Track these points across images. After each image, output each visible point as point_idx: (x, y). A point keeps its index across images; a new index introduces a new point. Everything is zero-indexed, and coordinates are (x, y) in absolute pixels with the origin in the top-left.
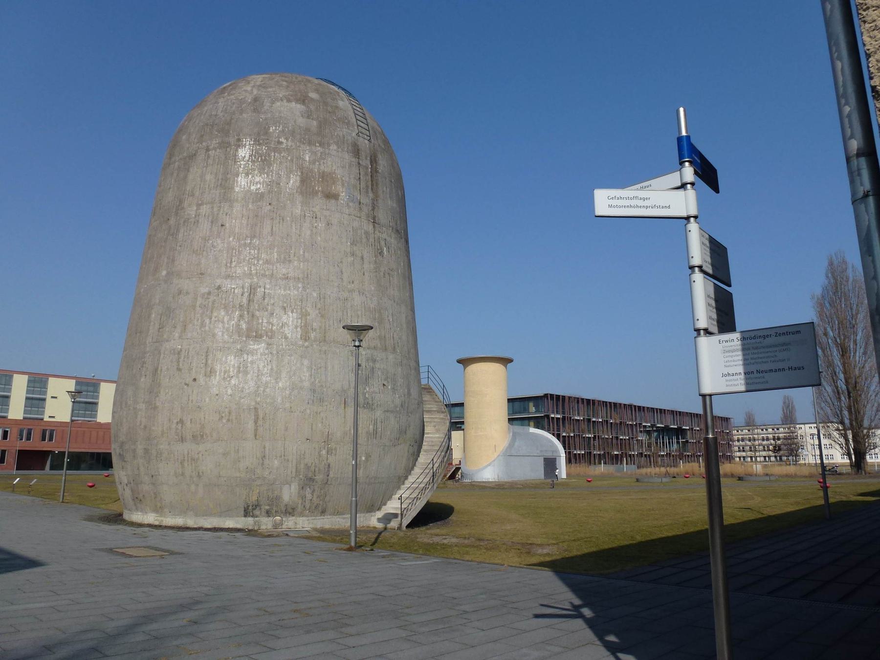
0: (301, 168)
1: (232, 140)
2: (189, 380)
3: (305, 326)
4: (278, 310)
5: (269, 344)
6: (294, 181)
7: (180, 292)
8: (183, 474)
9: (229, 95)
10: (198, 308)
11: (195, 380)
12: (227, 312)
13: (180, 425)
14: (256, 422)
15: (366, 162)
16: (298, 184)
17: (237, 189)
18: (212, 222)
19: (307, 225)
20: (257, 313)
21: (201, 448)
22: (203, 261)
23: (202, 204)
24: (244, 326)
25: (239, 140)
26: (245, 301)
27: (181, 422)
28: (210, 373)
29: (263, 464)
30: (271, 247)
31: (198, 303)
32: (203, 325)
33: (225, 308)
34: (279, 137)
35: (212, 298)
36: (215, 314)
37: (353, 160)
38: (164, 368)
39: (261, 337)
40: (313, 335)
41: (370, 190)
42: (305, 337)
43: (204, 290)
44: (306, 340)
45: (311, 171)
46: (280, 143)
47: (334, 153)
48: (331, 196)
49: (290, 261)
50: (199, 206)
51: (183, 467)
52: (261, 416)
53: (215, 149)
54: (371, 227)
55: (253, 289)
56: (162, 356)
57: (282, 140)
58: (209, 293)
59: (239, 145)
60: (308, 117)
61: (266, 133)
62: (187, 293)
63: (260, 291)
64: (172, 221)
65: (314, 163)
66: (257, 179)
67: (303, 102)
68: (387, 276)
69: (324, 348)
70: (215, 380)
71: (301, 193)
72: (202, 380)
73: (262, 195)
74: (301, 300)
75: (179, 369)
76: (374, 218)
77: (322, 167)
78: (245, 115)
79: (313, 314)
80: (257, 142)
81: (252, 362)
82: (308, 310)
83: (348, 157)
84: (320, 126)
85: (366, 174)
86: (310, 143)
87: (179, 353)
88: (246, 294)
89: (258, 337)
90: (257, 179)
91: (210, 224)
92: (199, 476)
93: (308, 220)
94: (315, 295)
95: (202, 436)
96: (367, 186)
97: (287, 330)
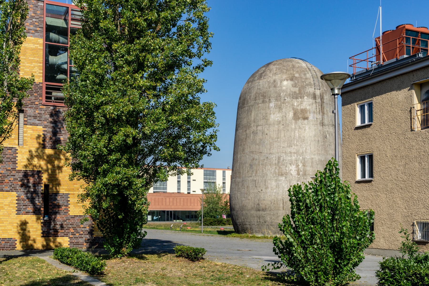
0: (293, 109)
1: (267, 100)
2: (260, 190)
3: (298, 170)
4: (289, 165)
5: (286, 177)
6: (291, 114)
7: (253, 159)
8: (260, 222)
9: (264, 79)
12: (271, 167)
14: (283, 204)
15: (319, 100)
16: (293, 116)
17: (271, 120)
19: (297, 132)
20: (281, 166)
23: (258, 126)
24: (277, 171)
25: (270, 100)
26: (277, 162)
27: (258, 204)
28: (267, 188)
30: (284, 142)
31: (261, 163)
32: (263, 171)
34: (284, 97)
35: (265, 161)
36: (267, 167)
37: (314, 101)
38: (251, 186)
39: (283, 175)
40: (301, 173)
41: (321, 112)
42: (298, 174)
43: (262, 158)
44: (298, 175)
45: (298, 109)
46: (285, 100)
47: (306, 100)
48: (306, 118)
49: (291, 146)
50: (257, 126)
51: (260, 219)
52: (285, 202)
53: (261, 103)
54: (322, 127)
55: (279, 158)
57: (286, 98)
58: (264, 160)
59: (270, 101)
60: (295, 87)
61: (280, 96)
62: (256, 160)
63: (282, 158)
64: (248, 132)
65: (298, 106)
66: (278, 115)
67: (292, 80)
68: (329, 146)
69: (305, 178)
70: (269, 190)
71: (294, 119)
72: (264, 190)
73: (280, 121)
74: (296, 161)
75: (256, 187)
76: (323, 123)
77: (302, 107)
78: (271, 89)
79: (301, 165)
80: (277, 100)
81: (281, 184)
82: (299, 164)
83: (311, 101)
84: (300, 90)
85: (319, 105)
86: (297, 98)
87: (255, 181)
88: (277, 160)
89: (282, 175)
90: (278, 115)
92: (265, 222)
93: (297, 129)
94: (301, 158)
96: (320, 111)
97: (291, 172)
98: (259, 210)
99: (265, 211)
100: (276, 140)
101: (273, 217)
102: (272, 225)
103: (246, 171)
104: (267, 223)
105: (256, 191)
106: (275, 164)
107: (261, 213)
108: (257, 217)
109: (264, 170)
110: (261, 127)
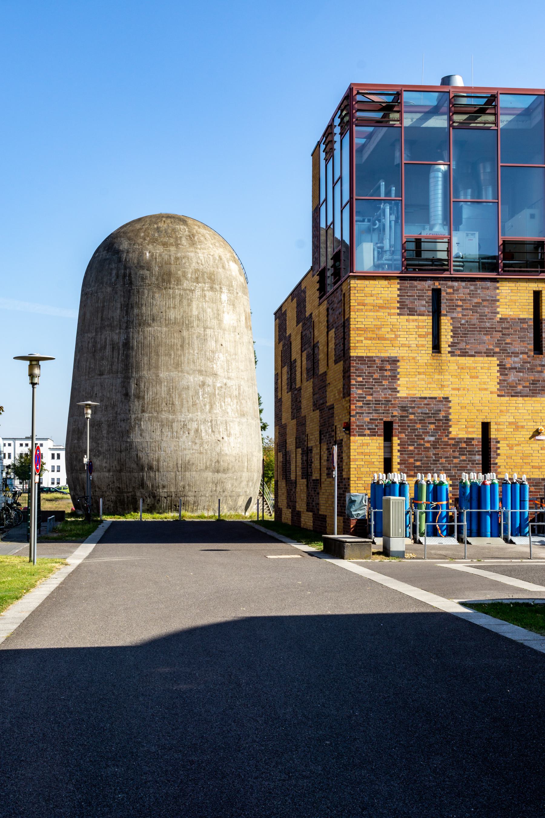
2: (220, 439)
8: (216, 491)
10: (217, 396)
11: (223, 438)
13: (217, 463)
18: (216, 342)
21: (226, 476)
22: (215, 366)
25: (221, 288)
27: (218, 462)
28: (229, 435)
29: (248, 485)
31: (217, 393)
32: (221, 407)
33: (230, 397)
35: (223, 390)
43: (218, 385)
51: (216, 487)
56: (200, 422)
58: (221, 387)
70: (232, 439)
72: (226, 438)
87: (211, 421)
91: (215, 343)
95: (228, 470)
98: (218, 472)
99: (226, 474)
100: (234, 357)
101: (236, 484)
102: (230, 496)
103: (191, 403)
104: (226, 493)
105: (213, 438)
106: (236, 396)
107: (220, 475)
108: (213, 482)
109: (223, 404)
110: (212, 330)
